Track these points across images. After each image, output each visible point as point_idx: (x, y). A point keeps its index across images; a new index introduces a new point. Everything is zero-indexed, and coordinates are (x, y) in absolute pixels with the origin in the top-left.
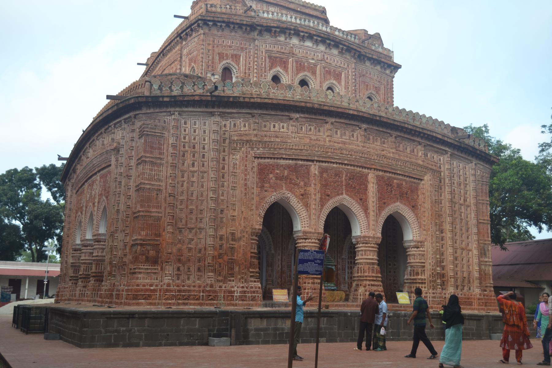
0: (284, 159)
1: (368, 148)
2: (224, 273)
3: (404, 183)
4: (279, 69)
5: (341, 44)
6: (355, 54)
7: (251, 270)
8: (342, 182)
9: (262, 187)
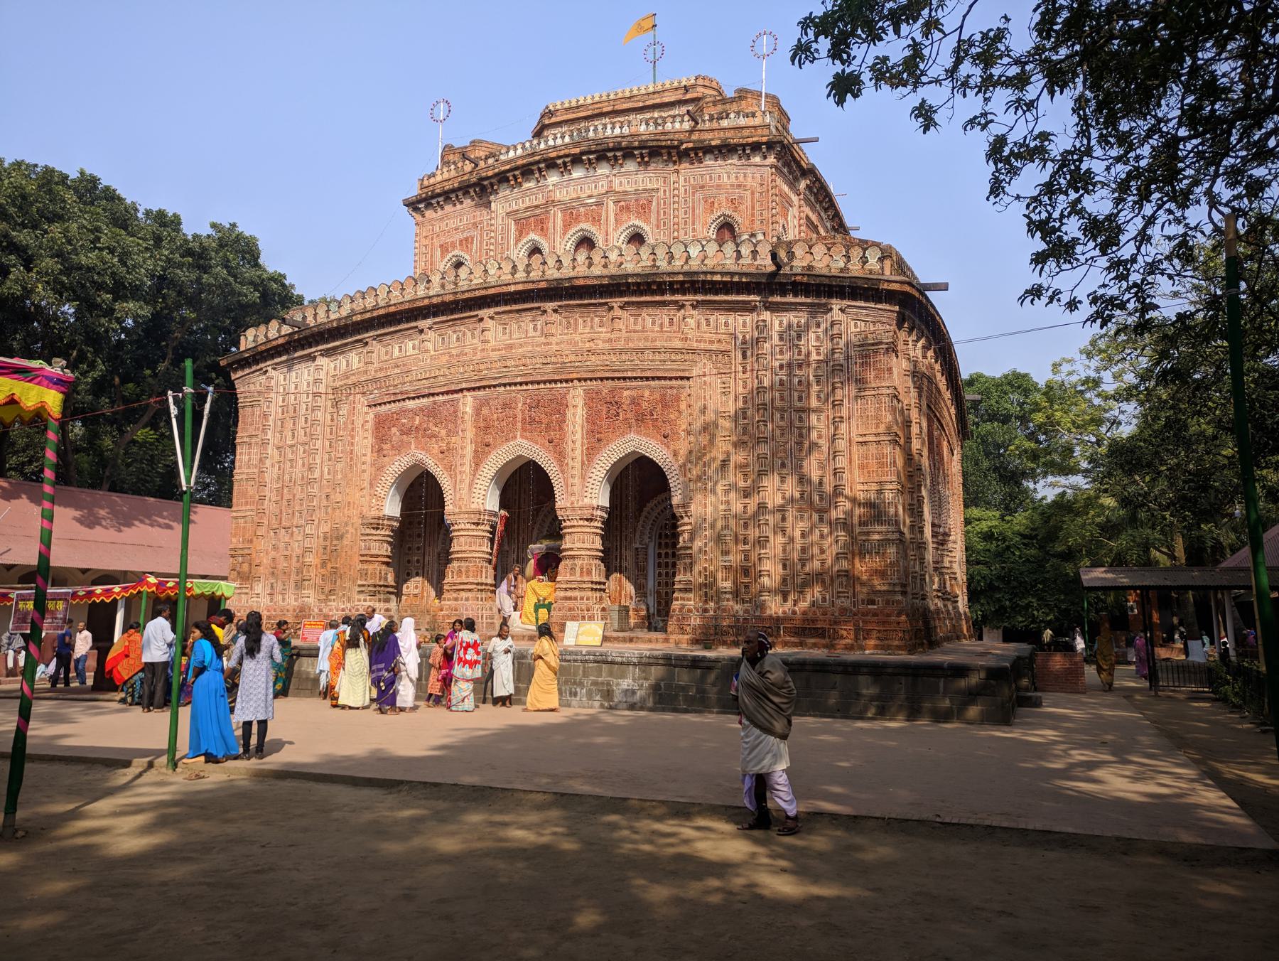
0: (413, 398)
1: (557, 344)
2: (327, 590)
3: (647, 393)
4: (532, 236)
5: (636, 148)
6: (669, 154)
7: (360, 582)
8: (515, 417)
9: (380, 450)
